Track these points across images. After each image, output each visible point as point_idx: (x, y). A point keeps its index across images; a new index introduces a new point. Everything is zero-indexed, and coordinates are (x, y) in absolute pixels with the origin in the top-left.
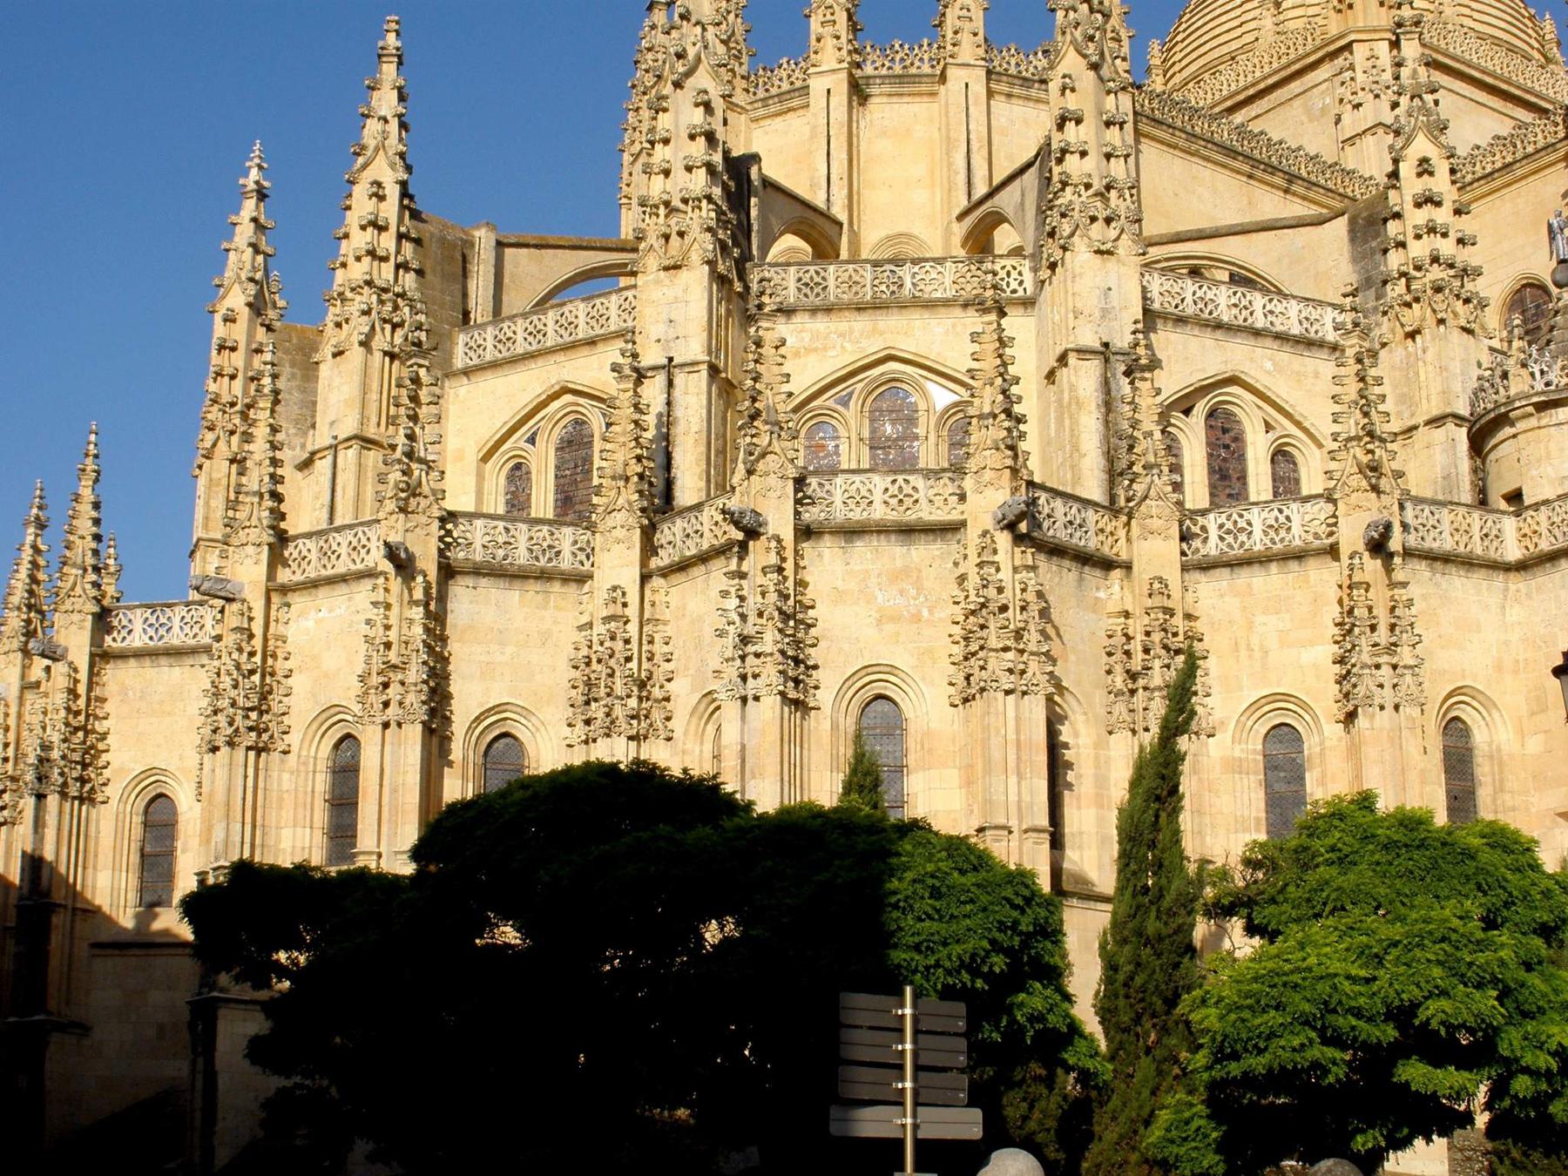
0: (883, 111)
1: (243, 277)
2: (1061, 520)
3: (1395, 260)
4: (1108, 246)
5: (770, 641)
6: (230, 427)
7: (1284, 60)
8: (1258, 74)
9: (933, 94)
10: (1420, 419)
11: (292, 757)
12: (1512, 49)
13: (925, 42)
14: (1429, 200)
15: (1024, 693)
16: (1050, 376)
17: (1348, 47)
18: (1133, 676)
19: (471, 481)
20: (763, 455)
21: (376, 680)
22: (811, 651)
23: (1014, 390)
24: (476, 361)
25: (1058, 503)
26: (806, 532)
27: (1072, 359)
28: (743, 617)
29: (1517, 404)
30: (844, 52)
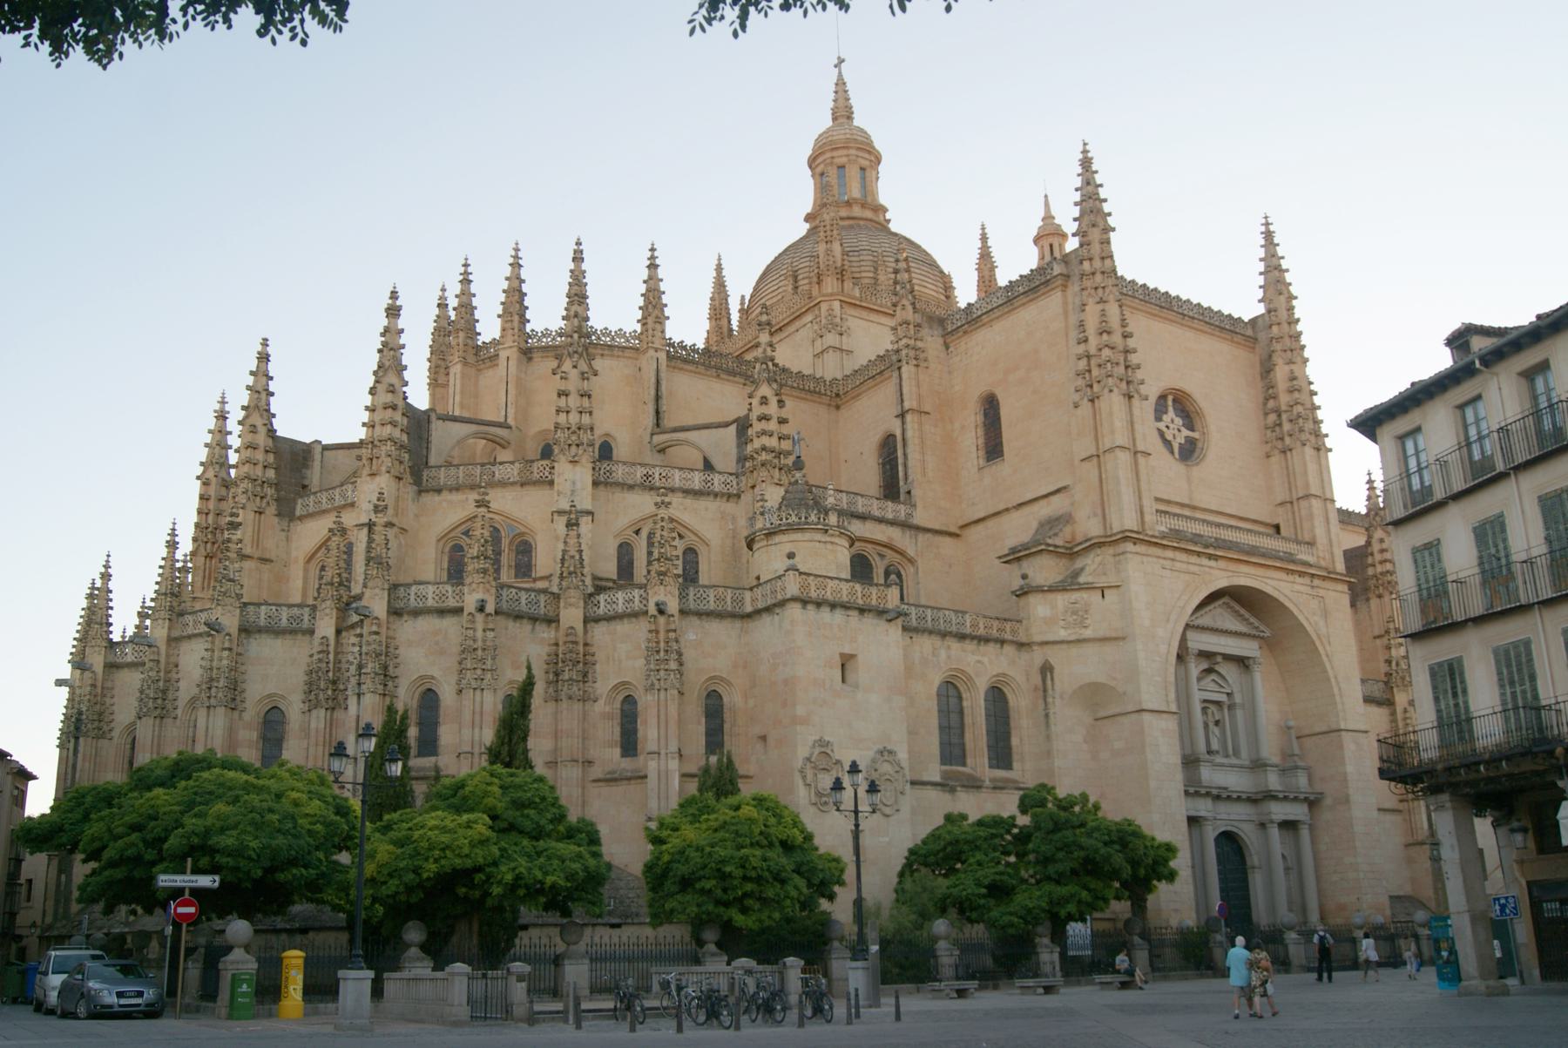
1: (214, 461)
2: (523, 601)
3: (749, 448)
4: (576, 459)
5: (370, 667)
6: (205, 540)
11: (178, 721)
14: (764, 418)
19: (301, 574)
21: (204, 687)
24: (305, 513)
28: (360, 654)
30: (516, 337)
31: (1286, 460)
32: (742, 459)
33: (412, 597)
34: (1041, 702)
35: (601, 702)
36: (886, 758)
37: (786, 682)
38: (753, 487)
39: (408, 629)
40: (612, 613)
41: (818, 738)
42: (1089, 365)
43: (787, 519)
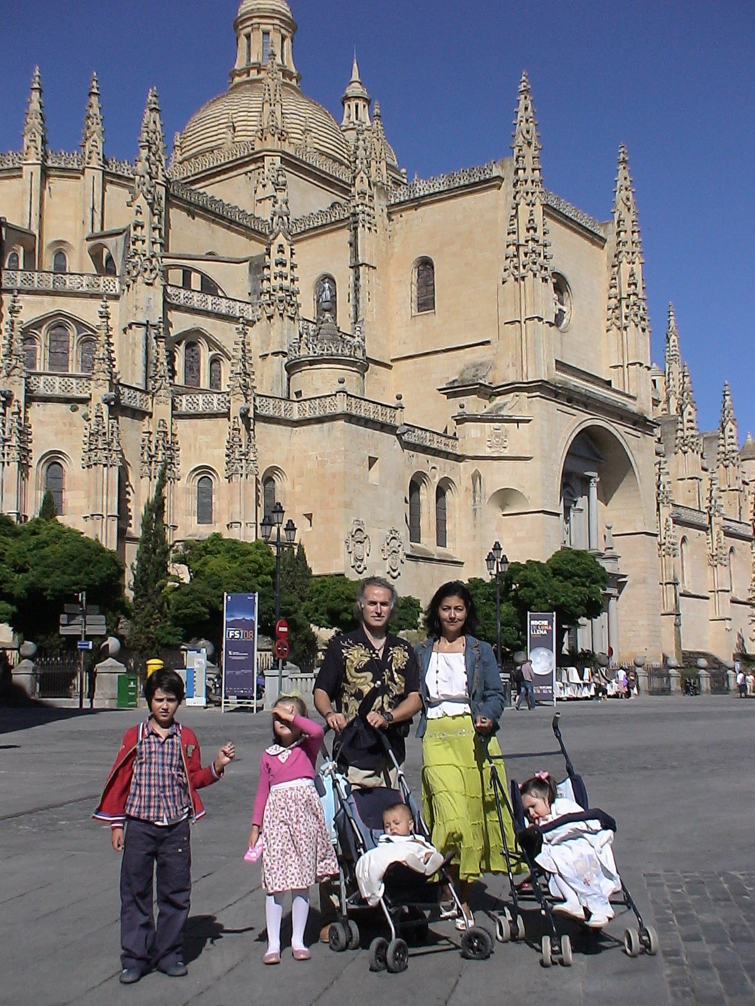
0: (56, 184)
4: (151, 281)
7: (234, 157)
8: (223, 162)
9: (79, 178)
10: (270, 351)
12: (335, 160)
13: (76, 152)
15: (111, 466)
16: (125, 330)
17: (262, 158)
18: (151, 457)
20: (15, 367)
22: (29, 445)
23: (112, 348)
25: (126, 390)
26: (31, 398)
27: (134, 327)
29: (303, 359)
30: (40, 156)
31: (622, 334)
32: (256, 292)
33: (41, 385)
34: (470, 501)
35: (184, 480)
36: (393, 536)
37: (334, 476)
38: (270, 318)
39: (37, 412)
40: (192, 411)
41: (356, 519)
42: (518, 250)
43: (328, 350)
